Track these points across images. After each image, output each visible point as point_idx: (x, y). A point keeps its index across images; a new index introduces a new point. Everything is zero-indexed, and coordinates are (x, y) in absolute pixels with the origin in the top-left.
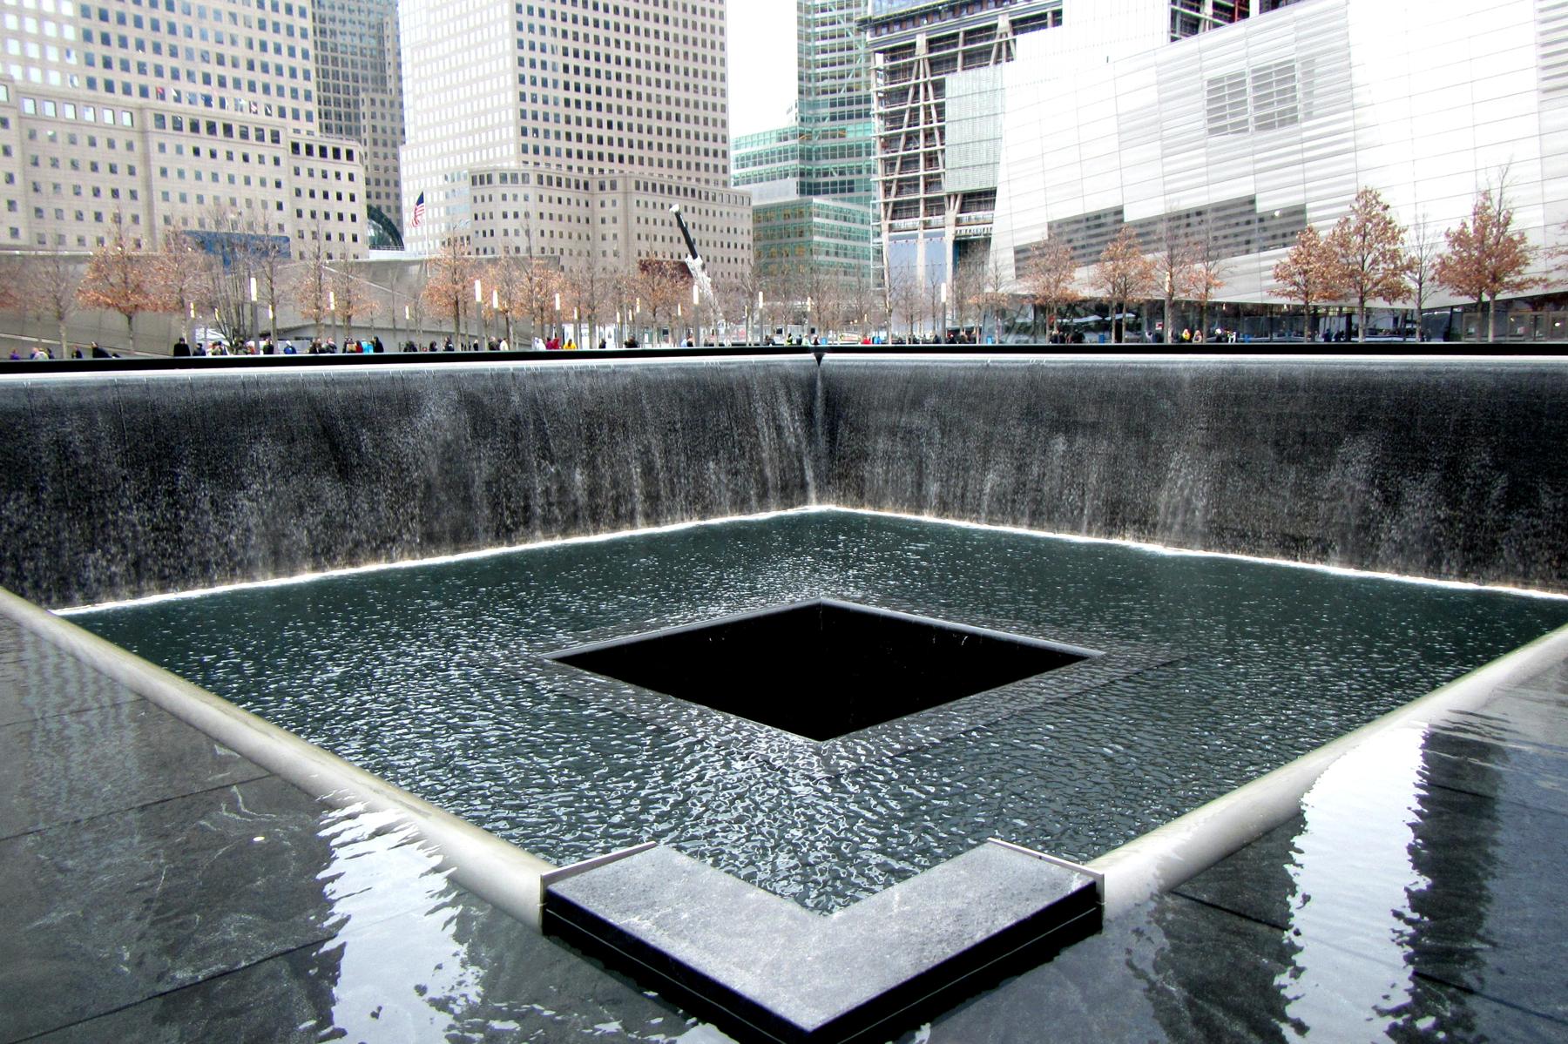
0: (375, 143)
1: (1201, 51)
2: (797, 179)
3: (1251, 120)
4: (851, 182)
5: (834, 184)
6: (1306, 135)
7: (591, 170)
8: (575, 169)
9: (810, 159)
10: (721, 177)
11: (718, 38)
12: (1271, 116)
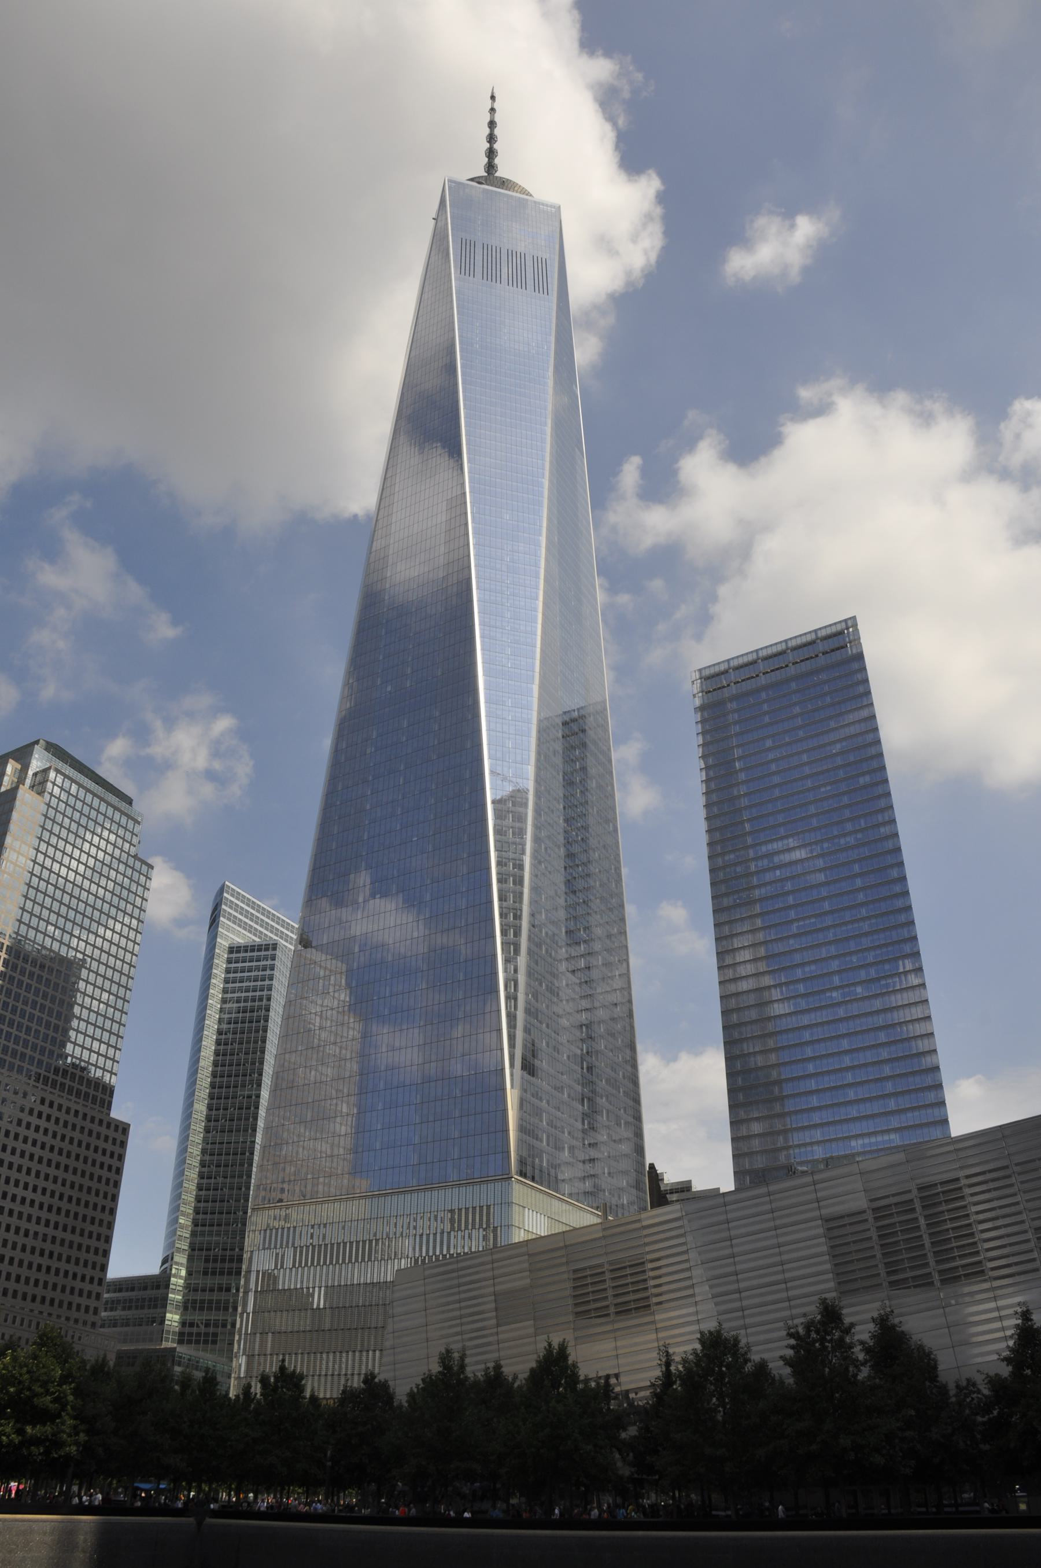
5: (198, 1334)
11: (110, 1189)
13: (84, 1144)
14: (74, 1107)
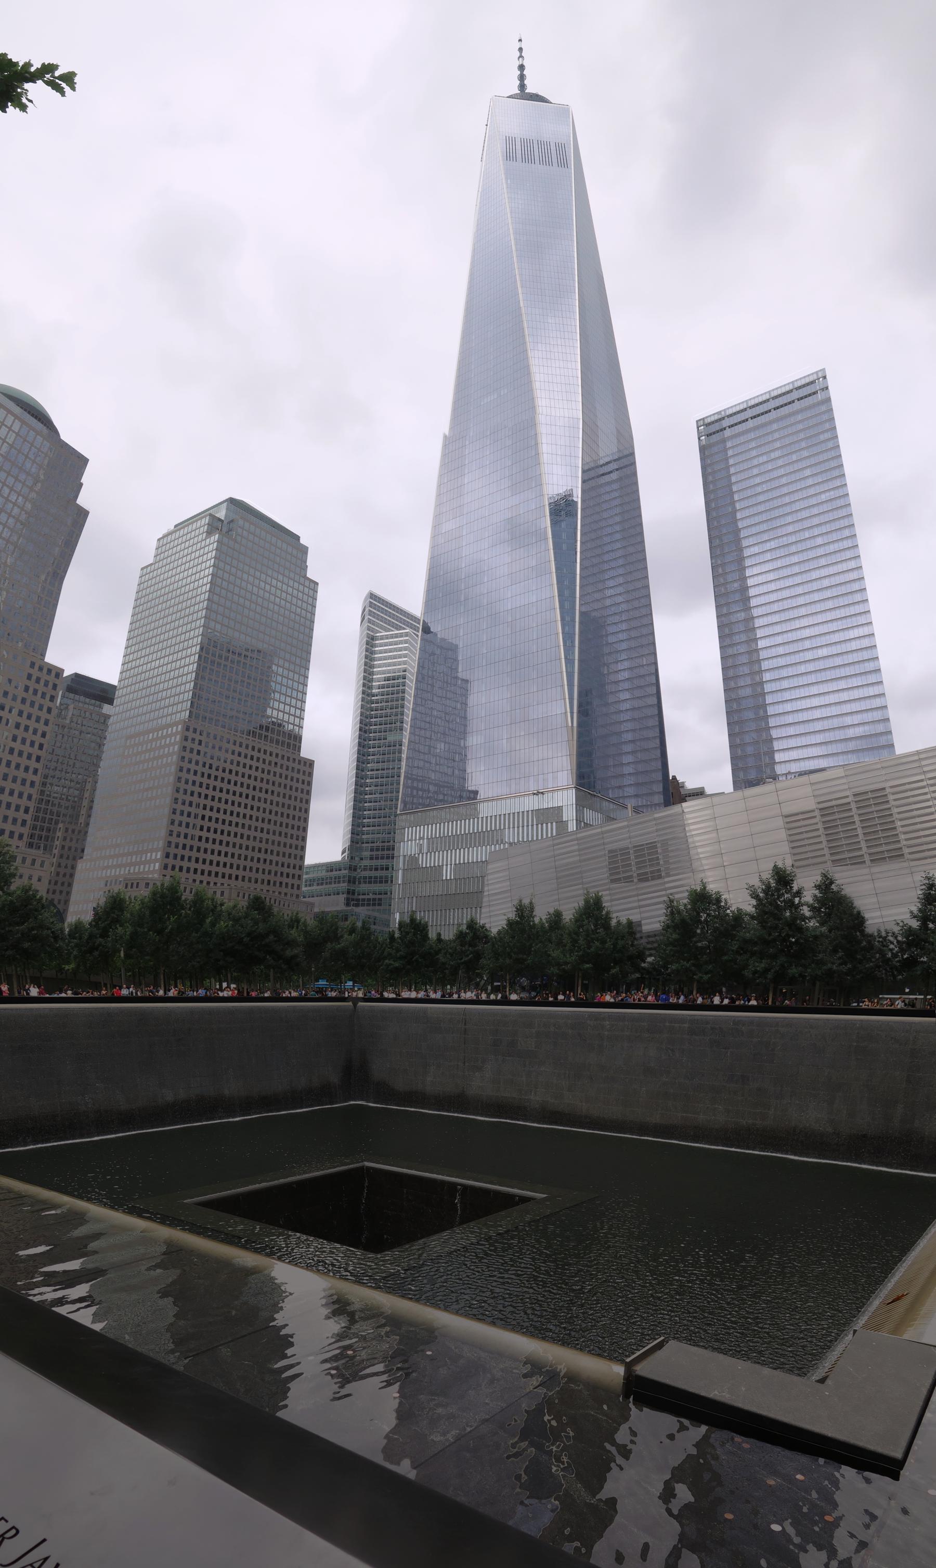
0: (61, 856)
1: (602, 833)
2: (345, 896)
3: (635, 875)
4: (380, 899)
5: (369, 900)
6: (667, 885)
7: (208, 883)
8: (198, 882)
9: (354, 883)
10: (295, 891)
11: (304, 806)
12: (646, 873)
13: (284, 776)
14: (275, 751)
